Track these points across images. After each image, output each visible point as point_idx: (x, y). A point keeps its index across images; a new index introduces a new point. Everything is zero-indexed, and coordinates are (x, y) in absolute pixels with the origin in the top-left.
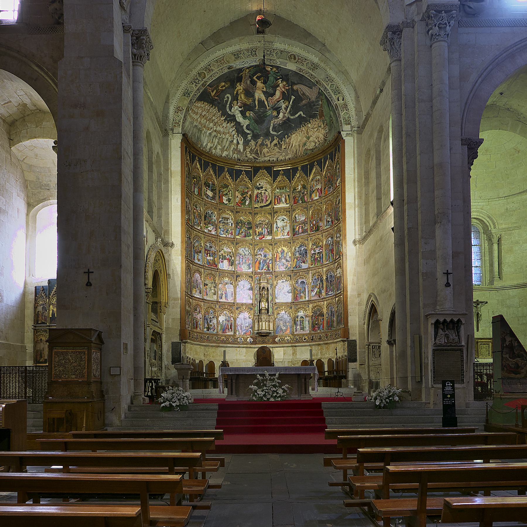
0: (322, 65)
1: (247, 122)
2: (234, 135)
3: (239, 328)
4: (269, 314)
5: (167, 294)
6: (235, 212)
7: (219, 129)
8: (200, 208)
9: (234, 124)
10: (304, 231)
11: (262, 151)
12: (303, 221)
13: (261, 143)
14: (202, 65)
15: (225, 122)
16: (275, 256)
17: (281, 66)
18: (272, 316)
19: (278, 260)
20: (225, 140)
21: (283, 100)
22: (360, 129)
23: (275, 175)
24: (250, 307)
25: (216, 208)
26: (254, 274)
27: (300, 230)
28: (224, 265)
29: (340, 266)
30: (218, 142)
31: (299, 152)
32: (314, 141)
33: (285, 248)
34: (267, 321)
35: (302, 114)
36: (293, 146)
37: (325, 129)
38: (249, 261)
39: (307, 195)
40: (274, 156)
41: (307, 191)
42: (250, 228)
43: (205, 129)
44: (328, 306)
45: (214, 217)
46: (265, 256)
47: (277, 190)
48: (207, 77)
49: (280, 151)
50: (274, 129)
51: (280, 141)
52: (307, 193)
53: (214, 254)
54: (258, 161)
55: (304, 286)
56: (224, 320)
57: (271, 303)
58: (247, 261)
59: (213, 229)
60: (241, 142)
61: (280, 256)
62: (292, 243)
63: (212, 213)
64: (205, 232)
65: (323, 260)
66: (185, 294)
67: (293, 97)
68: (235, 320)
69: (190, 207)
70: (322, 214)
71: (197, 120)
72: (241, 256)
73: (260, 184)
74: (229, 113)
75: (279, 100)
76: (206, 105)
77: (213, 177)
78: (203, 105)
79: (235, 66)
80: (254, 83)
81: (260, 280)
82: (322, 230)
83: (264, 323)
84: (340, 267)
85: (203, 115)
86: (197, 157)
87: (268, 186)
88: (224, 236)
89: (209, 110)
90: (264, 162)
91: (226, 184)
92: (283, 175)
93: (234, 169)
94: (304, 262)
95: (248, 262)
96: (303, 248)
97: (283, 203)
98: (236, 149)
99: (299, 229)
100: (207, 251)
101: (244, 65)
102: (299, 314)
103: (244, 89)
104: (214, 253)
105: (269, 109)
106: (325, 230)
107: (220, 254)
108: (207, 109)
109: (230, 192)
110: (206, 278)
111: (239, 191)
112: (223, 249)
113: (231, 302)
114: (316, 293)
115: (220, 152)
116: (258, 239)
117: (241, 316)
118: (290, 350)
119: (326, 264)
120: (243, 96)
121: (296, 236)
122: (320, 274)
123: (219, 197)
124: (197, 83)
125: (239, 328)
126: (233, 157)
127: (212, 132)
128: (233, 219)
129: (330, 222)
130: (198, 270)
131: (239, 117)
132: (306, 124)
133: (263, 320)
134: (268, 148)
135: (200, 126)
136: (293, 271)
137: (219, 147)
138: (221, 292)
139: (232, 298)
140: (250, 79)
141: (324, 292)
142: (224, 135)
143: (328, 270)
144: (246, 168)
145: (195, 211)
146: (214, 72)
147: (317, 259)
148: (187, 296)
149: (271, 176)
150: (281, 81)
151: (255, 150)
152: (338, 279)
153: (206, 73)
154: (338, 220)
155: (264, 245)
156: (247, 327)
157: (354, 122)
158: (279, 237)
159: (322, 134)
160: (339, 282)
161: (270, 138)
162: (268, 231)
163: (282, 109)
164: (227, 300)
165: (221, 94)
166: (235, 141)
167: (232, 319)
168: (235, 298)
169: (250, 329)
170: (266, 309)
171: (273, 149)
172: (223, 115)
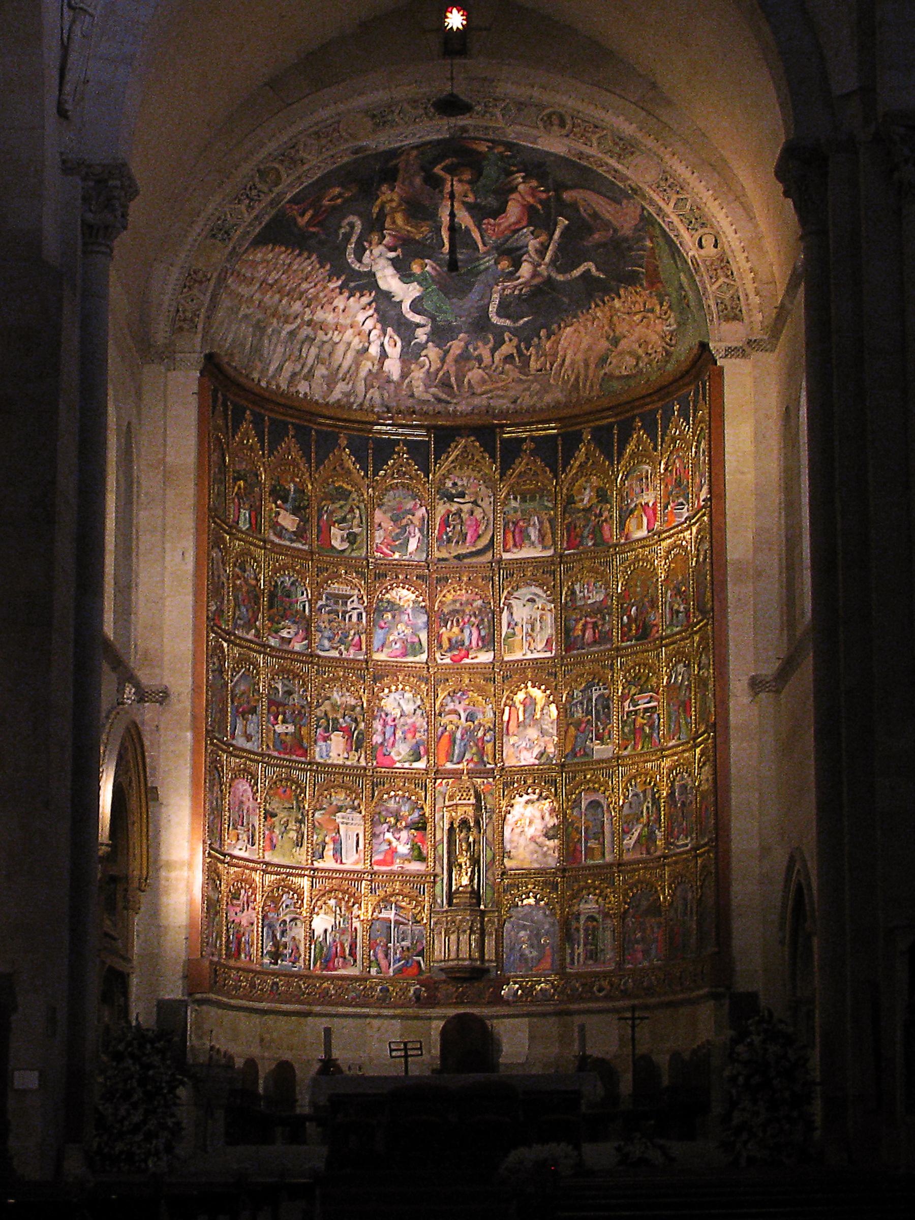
1: (412, 291)
2: (370, 332)
7: (320, 315)
9: (371, 299)
11: (465, 376)
13: (458, 352)
14: (272, 146)
15: (341, 293)
20: (341, 348)
27: (589, 634)
30: (317, 356)
33: (537, 694)
38: (418, 735)
40: (500, 393)
43: (275, 320)
46: (471, 718)
47: (514, 504)
53: (298, 717)
56: (330, 929)
58: (409, 736)
59: (296, 634)
60: (394, 352)
61: (521, 719)
63: (293, 584)
64: (270, 647)
69: (222, 572)
73: (455, 484)
74: (356, 266)
77: (299, 469)
78: (271, 255)
81: (451, 798)
85: (270, 282)
86: (248, 412)
89: (290, 265)
91: (341, 487)
95: (414, 737)
98: (377, 373)
103: (401, 198)
107: (319, 712)
108: (284, 264)
109: (357, 511)
111: (384, 508)
112: (329, 698)
113: (354, 872)
116: (448, 661)
118: (551, 1026)
127: (299, 327)
128: (365, 598)
131: (389, 279)
134: (484, 369)
142: (336, 333)
145: (238, 582)
151: (441, 373)
161: (491, 337)
162: (483, 633)
164: (341, 863)
166: (374, 350)
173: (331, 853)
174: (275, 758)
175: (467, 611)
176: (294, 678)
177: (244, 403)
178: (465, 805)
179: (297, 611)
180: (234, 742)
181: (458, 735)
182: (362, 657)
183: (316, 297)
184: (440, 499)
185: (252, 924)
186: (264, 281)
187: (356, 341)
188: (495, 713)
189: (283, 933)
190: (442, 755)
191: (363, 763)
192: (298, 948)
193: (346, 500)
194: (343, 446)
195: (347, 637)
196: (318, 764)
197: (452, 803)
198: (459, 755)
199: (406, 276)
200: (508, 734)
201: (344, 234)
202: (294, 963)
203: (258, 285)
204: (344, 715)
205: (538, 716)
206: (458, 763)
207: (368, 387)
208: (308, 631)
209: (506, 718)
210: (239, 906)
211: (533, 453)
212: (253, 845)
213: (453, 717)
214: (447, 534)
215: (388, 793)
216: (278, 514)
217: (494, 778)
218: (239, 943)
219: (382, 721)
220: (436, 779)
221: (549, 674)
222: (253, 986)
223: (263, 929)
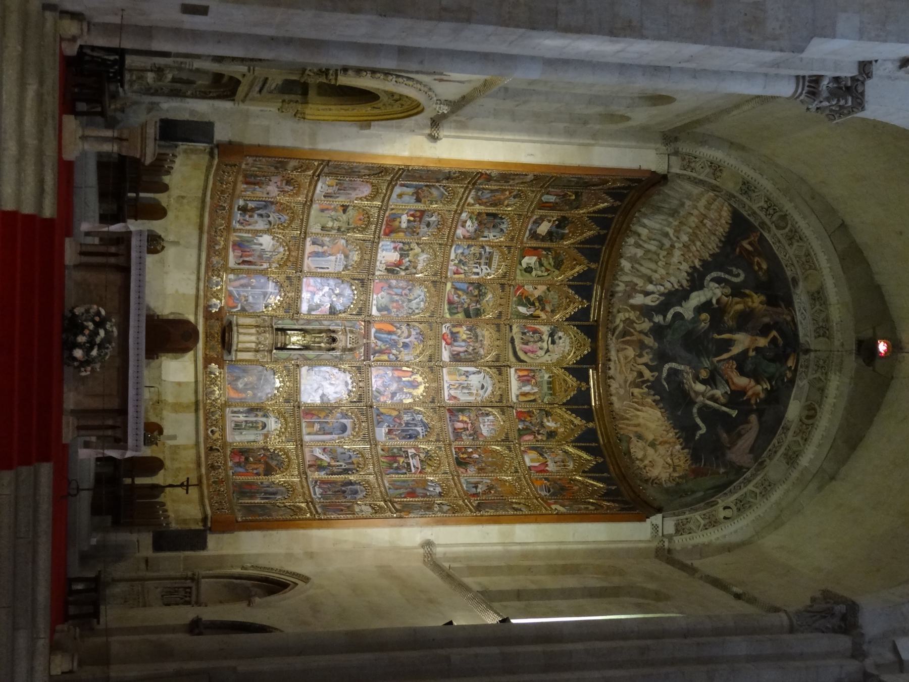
0: (795, 474)
3: (243, 281)
4: (274, 351)
5: (326, 118)
6: (503, 281)
7: (677, 253)
8: (514, 204)
10: (457, 434)
11: (630, 346)
12: (479, 431)
17: (794, 389)
18: (269, 357)
19: (397, 374)
20: (653, 266)
21: (729, 393)
22: (665, 555)
23: (579, 371)
24: (291, 306)
25: (512, 239)
26: (367, 319)
27: (460, 425)
28: (387, 254)
29: (377, 511)
31: (623, 424)
32: (645, 456)
33: (421, 390)
35: (701, 432)
36: (638, 413)
37: (669, 481)
38: (395, 310)
39: (534, 440)
40: (618, 368)
41: (542, 440)
43: (676, 223)
44: (289, 485)
45: (495, 234)
46: (406, 345)
47: (546, 376)
48: (779, 233)
49: (629, 382)
50: (673, 372)
51: (649, 384)
52: (537, 441)
54: (610, 335)
56: (262, 248)
57: (299, 357)
59: (468, 231)
60: (648, 301)
61: (404, 379)
62: (432, 405)
63: (502, 230)
64: (461, 214)
65: (393, 473)
66: (323, 161)
67: (734, 413)
68: (264, 273)
69: (517, 182)
70: (492, 472)
71: (696, 207)
73: (560, 338)
74: (708, 278)
75: (730, 383)
76: (723, 228)
77: (578, 236)
78: (723, 222)
79: (798, 292)
80: (764, 331)
81: (351, 332)
82: (457, 472)
83: (253, 338)
84: (376, 513)
85: (705, 221)
86: (620, 204)
88: (453, 256)
89: (715, 234)
90: (607, 350)
92: (579, 389)
93: (593, 283)
94: (390, 432)
95: (394, 307)
96: (420, 431)
97: (520, 388)
98: (635, 289)
99: (462, 422)
100: (419, 216)
101: (799, 310)
104: (414, 232)
105: (712, 363)
106: (459, 480)
107: (414, 245)
109: (546, 274)
110: (361, 210)
112: (423, 251)
113: (302, 265)
114: (318, 458)
115: (629, 255)
116: (444, 331)
117: (271, 287)
119: (382, 480)
120: (740, 307)
121: (448, 415)
122: (362, 468)
123: (535, 249)
124: (767, 210)
125: (243, 281)
126: (620, 283)
127: (670, 239)
129: (474, 489)
130: (378, 192)
131: (698, 299)
132: (681, 440)
133: (262, 339)
134: (634, 358)
135: (682, 213)
136: (371, 407)
137: (640, 253)
138: (328, 243)
139: (313, 266)
140: (772, 323)
141: (322, 475)
142: (664, 264)
143: (369, 486)
144: (595, 310)
145: (507, 193)
146: (787, 247)
147: (395, 462)
148: (319, 165)
149: (578, 362)
150: (766, 388)
151: (632, 330)
152: (348, 507)
153: (787, 230)
154: (479, 507)
155: (430, 343)
156: (246, 300)
157: (680, 541)
158: (447, 378)
159: (659, 474)
160: (342, 510)
161: (655, 363)
162: (462, 355)
163: (712, 389)
164: (309, 257)
165: (745, 260)
166: (650, 287)
167: (265, 266)
168: (314, 275)
169: (239, 305)
170: (286, 345)
171: (633, 368)
172: (704, 263)
173: (316, 250)
174: (384, 214)
175: (477, 344)
176: (438, 229)
177: (626, 201)
178: (347, 342)
179: (483, 232)
180: (398, 186)
181: (394, 337)
182: (449, 274)
183: (689, 250)
185: (268, 194)
186: (705, 217)
187: (659, 277)
188: (408, 361)
189: (261, 216)
190: (382, 326)
191: (377, 273)
192: (249, 225)
193: (554, 266)
195: (463, 264)
196: (378, 243)
197: (348, 331)
198: (380, 337)
199: (699, 309)
200: (393, 370)
201: (732, 271)
202: (239, 222)
203: (704, 212)
204: (410, 261)
206: (375, 337)
207: (627, 284)
208: (469, 238)
209: (405, 368)
210: (281, 184)
212: (324, 196)
213: (406, 334)
214: (528, 332)
215: (356, 289)
216: (549, 221)
217: (364, 360)
218: (255, 184)
220: (365, 321)
222: (223, 192)
223: (265, 201)
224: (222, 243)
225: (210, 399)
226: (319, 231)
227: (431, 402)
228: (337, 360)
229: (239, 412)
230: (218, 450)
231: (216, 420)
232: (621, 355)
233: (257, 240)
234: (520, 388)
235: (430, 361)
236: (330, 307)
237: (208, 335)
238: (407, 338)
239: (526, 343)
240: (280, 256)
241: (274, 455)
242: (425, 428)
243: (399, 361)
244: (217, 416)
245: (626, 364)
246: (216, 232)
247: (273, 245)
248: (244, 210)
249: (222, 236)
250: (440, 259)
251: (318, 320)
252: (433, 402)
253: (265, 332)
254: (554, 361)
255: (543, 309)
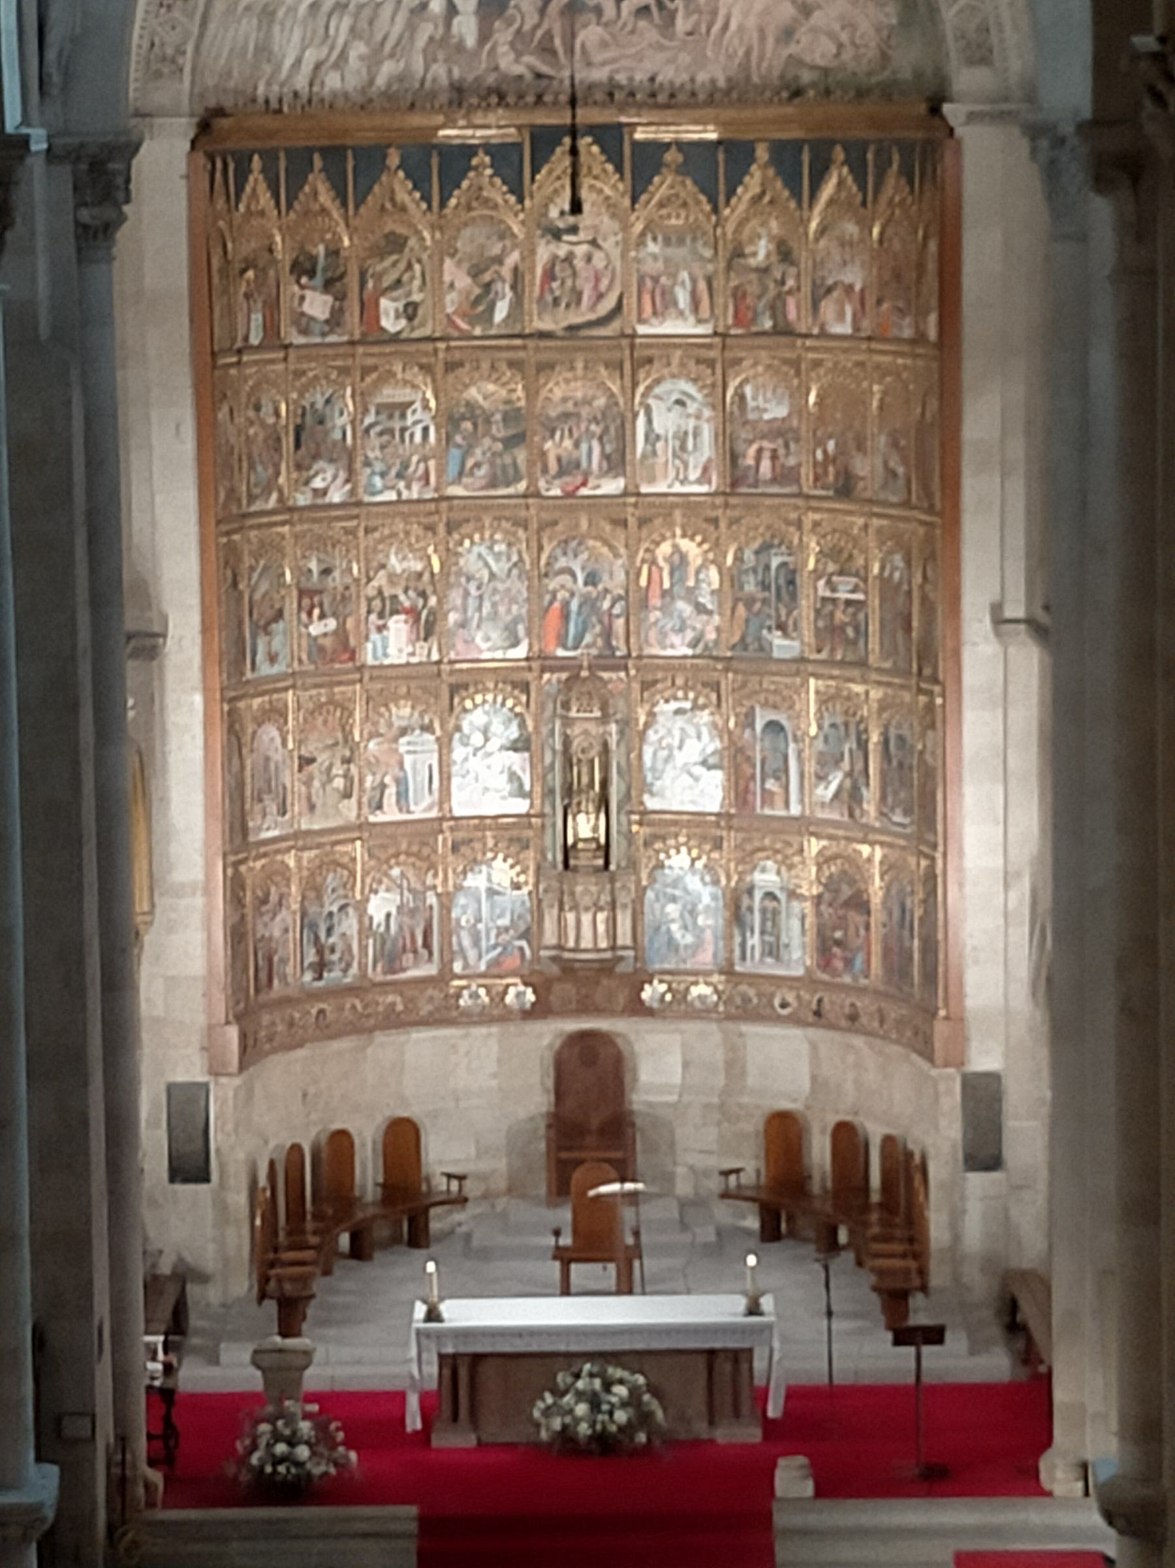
3: (466, 942)
6: (440, 369)
16: (643, 582)
19: (655, 601)
33: (690, 547)
34: (601, 909)
38: (515, 608)
42: (511, 442)
47: (652, 247)
55: (782, 745)
56: (394, 912)
61: (667, 585)
62: (723, 525)
72: (472, 588)
83: (586, 918)
87: (607, 223)
94: (781, 627)
95: (509, 611)
97: (681, 313)
102: (758, 877)
112: (383, 566)
121: (744, 490)
125: (466, 942)
133: (586, 901)
139: (427, 800)
155: (584, 524)
156: (507, 929)
164: (409, 812)
167: (432, 899)
169: (518, 943)
170: (599, 847)
173: (394, 798)
181: (574, 605)
184: (543, 236)
188: (627, 573)
189: (329, 931)
191: (435, 657)
192: (349, 948)
194: (393, 167)
198: (575, 638)
204: (406, 591)
205: (691, 583)
209: (643, 582)
211: (682, 170)
213: (565, 579)
214: (552, 291)
219: (461, 591)
221: (708, 520)
224: (390, 998)
225: (717, 1004)
226: (354, 800)
227: (717, 527)
228: (627, 731)
229: (743, 945)
230: (820, 1001)
231: (759, 995)
232: (597, 57)
233: (379, 926)
234: (681, 313)
235: (624, 524)
236: (516, 750)
237: (585, 1008)
238: (573, 575)
239: (579, 296)
240: (410, 874)
241: (831, 885)
242: (771, 546)
243: (627, 592)
244: (751, 992)
245: (618, 45)
246: (368, 1016)
247: (388, 890)
248: (320, 968)
249: (377, 1003)
250: (400, 526)
251: (541, 774)
252: (715, 522)
253: (572, 893)
254: (616, 225)
255: (499, 260)
